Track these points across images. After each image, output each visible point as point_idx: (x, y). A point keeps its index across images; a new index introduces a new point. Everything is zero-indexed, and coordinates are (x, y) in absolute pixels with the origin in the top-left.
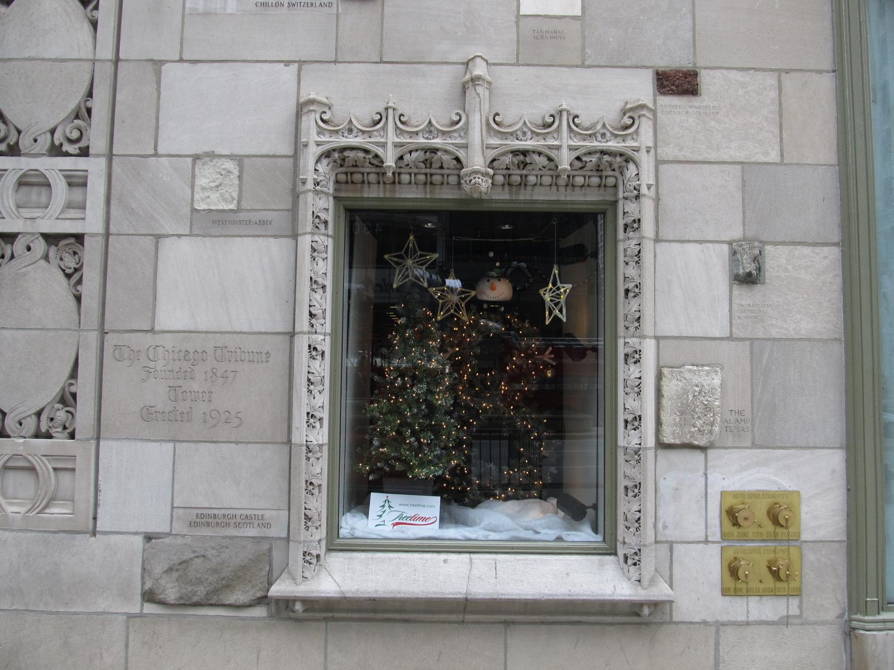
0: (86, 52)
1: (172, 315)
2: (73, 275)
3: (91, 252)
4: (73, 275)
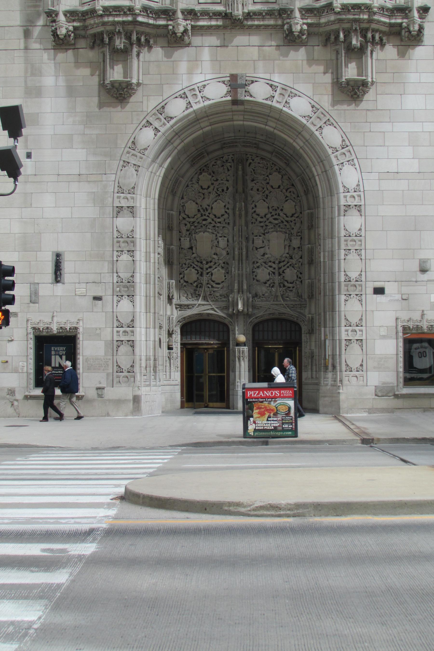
0: (361, 310)
1: (377, 352)
2: (361, 346)
3: (364, 342)
4: (361, 346)
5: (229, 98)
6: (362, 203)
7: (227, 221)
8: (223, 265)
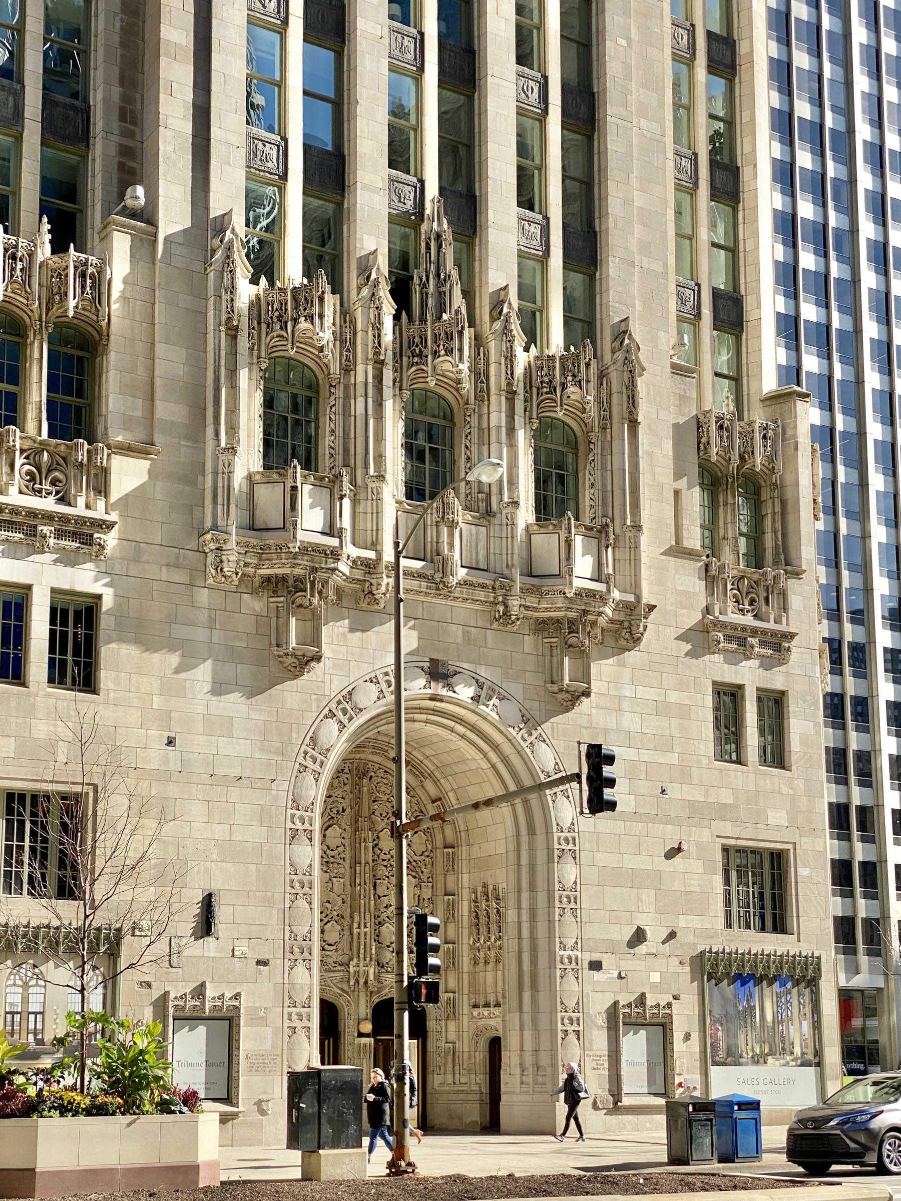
5: (429, 691)
6: (577, 848)
7: (342, 856)
8: (337, 918)
